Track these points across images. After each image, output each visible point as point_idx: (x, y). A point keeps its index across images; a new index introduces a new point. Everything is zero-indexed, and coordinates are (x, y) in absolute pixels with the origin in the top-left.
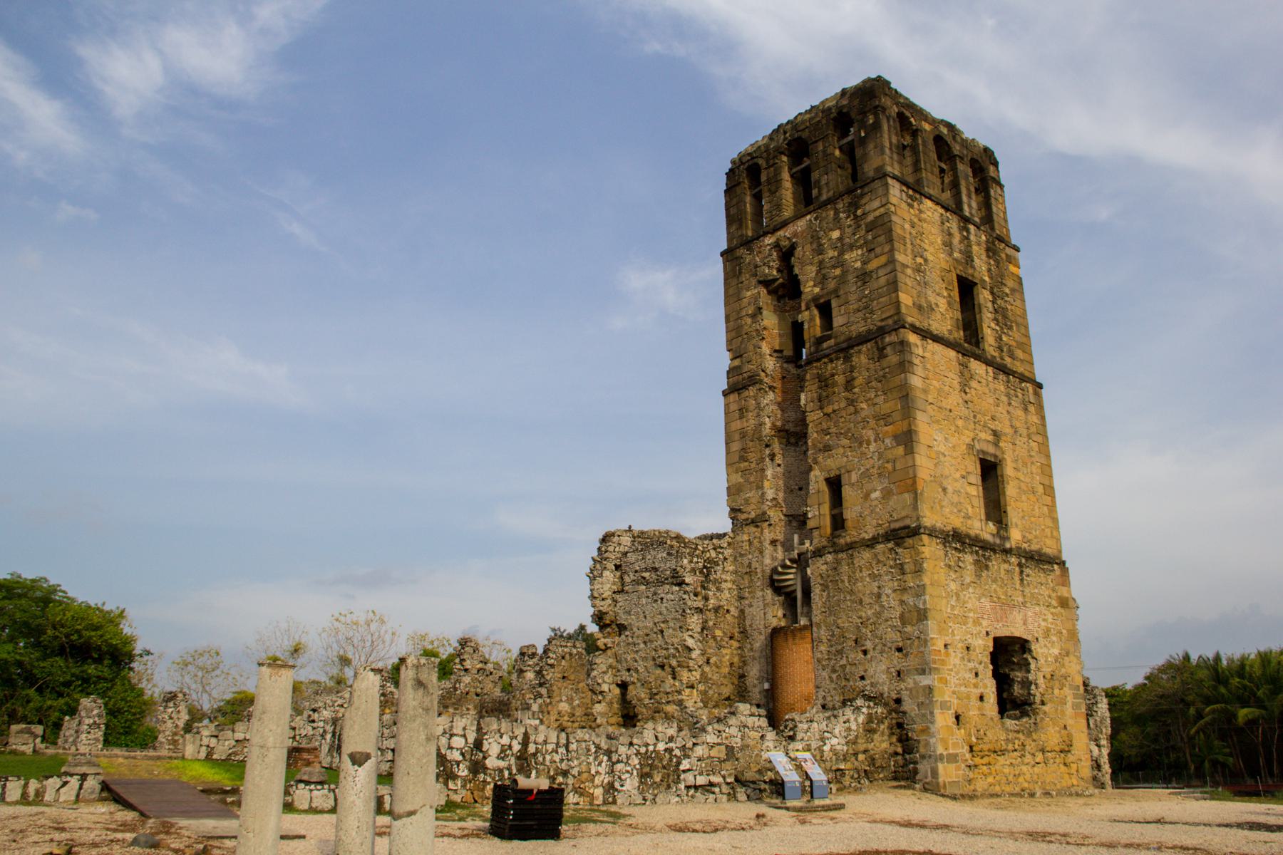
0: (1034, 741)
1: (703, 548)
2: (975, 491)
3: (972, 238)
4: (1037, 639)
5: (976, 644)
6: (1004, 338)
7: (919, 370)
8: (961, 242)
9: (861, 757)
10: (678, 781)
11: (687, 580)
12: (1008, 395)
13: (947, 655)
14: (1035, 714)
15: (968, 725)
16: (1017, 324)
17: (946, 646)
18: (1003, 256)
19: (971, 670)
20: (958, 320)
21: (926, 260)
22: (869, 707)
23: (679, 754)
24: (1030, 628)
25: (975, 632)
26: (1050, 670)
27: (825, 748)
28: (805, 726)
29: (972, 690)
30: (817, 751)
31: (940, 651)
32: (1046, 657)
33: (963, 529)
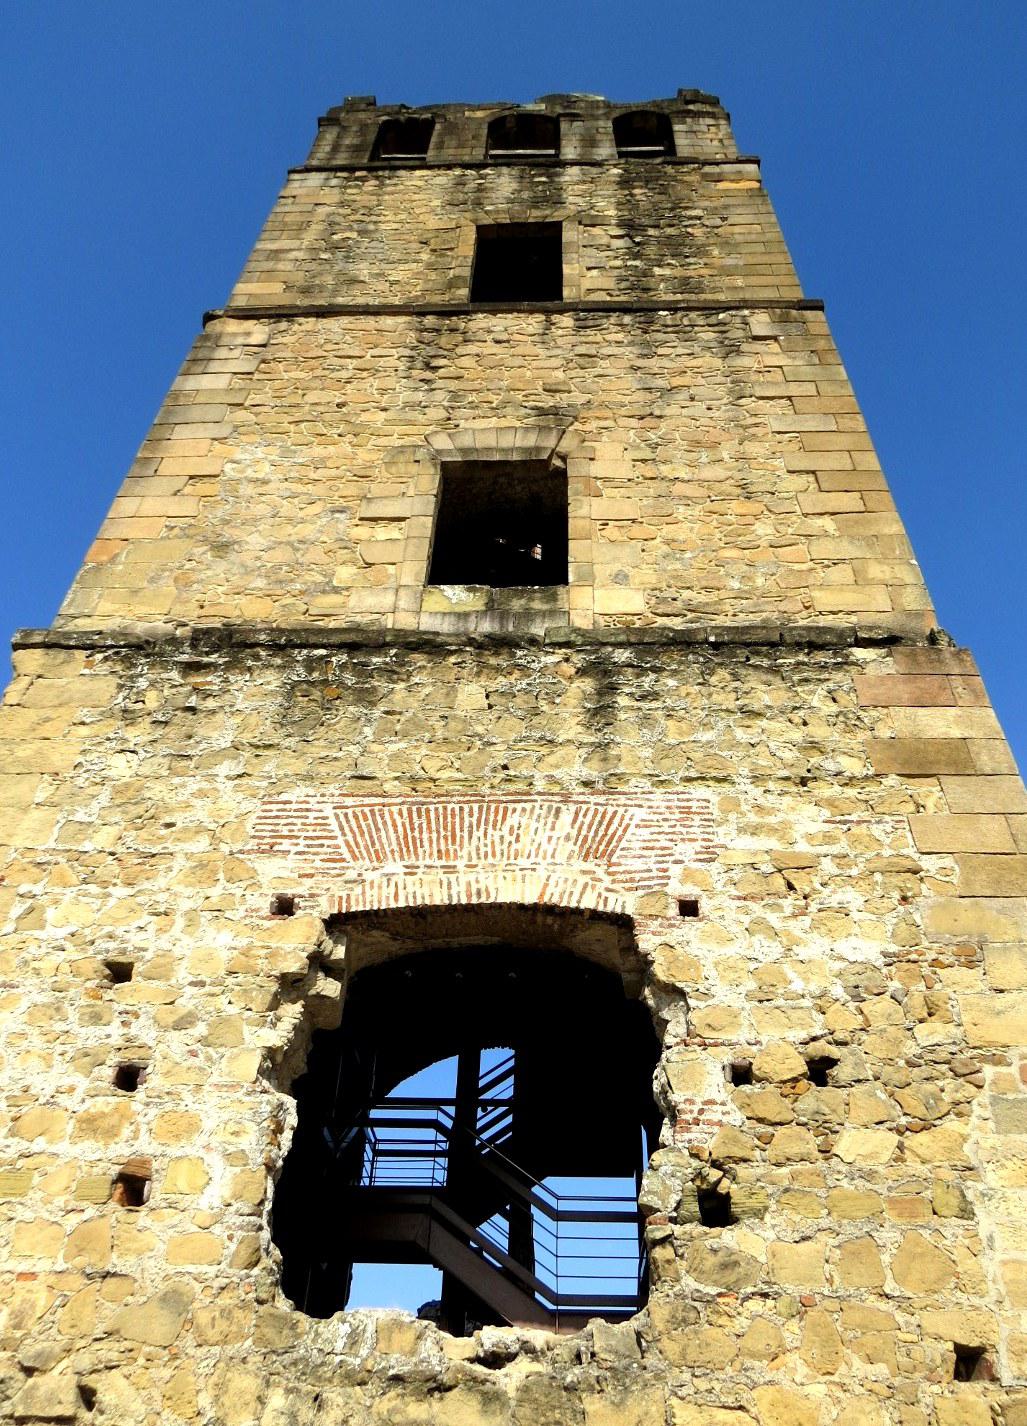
5: (186, 945)
19: (89, 1059)
24: (638, 865)
25: (185, 905)
29: (63, 1147)
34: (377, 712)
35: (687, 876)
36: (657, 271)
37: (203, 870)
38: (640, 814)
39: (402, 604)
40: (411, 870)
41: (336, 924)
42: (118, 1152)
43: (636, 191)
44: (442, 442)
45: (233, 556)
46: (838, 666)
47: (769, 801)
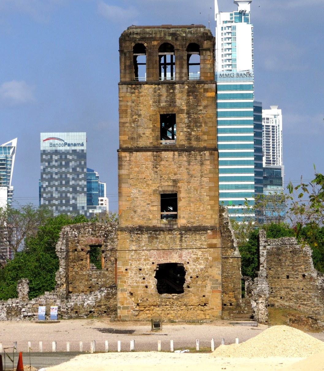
0: (180, 302)
1: (105, 226)
2: (156, 207)
3: (177, 91)
4: (188, 263)
5: (145, 267)
6: (193, 133)
7: (126, 167)
8: (167, 97)
9: (102, 307)
10: (21, 314)
11: (62, 248)
12: (189, 162)
13: (127, 273)
14: (182, 291)
15: (137, 297)
16: (206, 123)
17: (126, 270)
18: (202, 90)
19: (140, 277)
20: (157, 136)
21: (140, 116)
22: (108, 290)
23: (20, 306)
24: (184, 258)
25: (144, 263)
26: (196, 274)
27: (85, 304)
28: (75, 297)
30: (81, 305)
31: (122, 272)
32: (194, 270)
33: (145, 225)
34: (158, 240)
35: (188, 260)
36: (193, 133)
37: (145, 260)
38: (184, 253)
39: (159, 222)
40: (164, 259)
41: (157, 265)
42: (145, 284)
43: (191, 97)
44: (160, 189)
45: (137, 213)
46: (206, 233)
47: (197, 251)
